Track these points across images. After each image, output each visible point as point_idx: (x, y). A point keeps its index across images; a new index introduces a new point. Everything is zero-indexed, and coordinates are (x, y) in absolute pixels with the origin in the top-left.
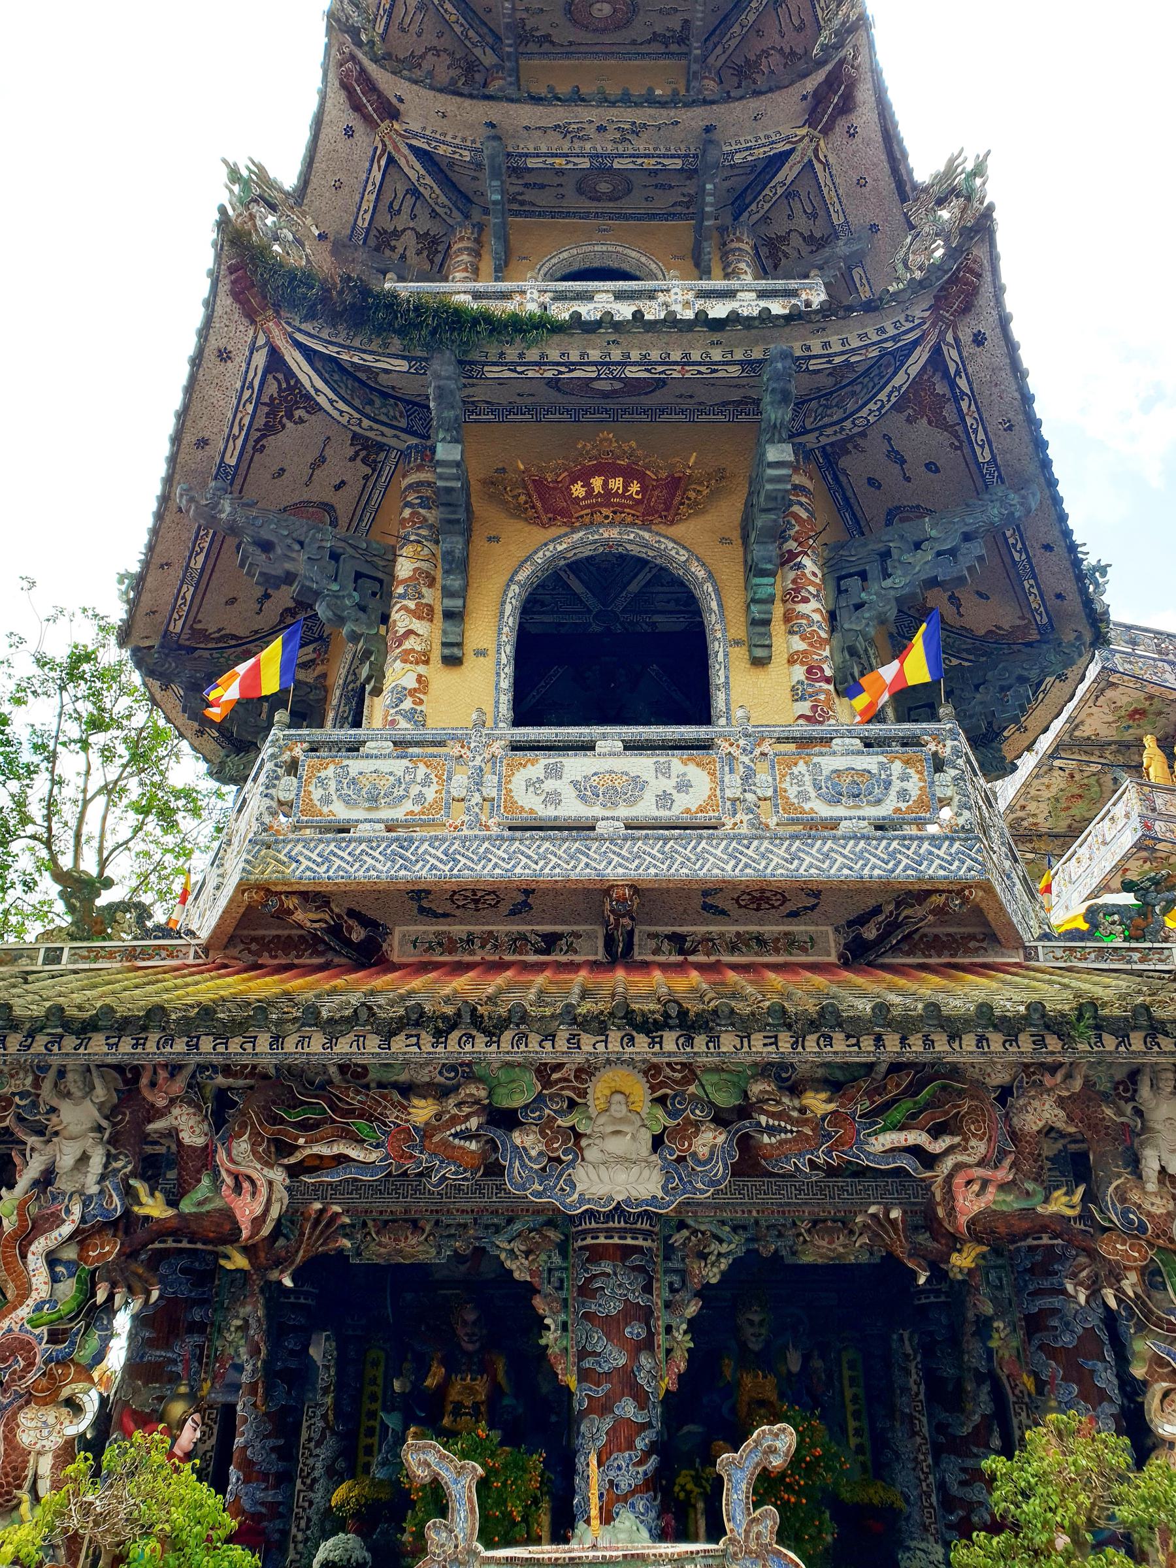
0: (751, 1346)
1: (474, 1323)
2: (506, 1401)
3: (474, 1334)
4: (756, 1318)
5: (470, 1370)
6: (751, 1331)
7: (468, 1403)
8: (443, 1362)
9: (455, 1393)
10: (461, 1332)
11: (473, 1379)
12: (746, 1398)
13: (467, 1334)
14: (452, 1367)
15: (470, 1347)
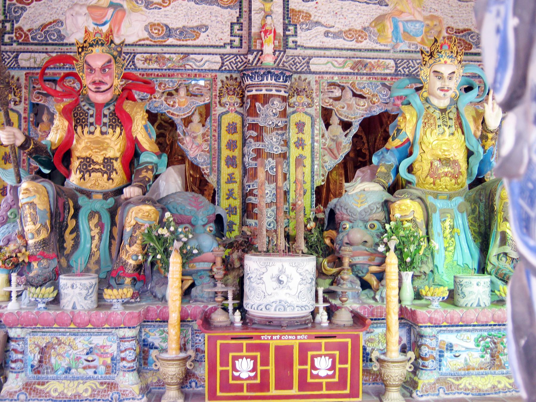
0: (435, 101)
1: (103, 69)
2: (144, 158)
3: (101, 83)
4: (445, 70)
5: (98, 120)
6: (438, 84)
7: (99, 158)
8: (66, 113)
9: (81, 147)
10: (87, 81)
11: (102, 133)
12: (428, 157)
13: (94, 83)
14: (76, 117)
15: (100, 98)
